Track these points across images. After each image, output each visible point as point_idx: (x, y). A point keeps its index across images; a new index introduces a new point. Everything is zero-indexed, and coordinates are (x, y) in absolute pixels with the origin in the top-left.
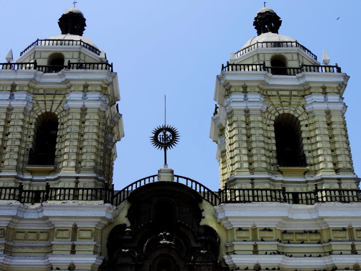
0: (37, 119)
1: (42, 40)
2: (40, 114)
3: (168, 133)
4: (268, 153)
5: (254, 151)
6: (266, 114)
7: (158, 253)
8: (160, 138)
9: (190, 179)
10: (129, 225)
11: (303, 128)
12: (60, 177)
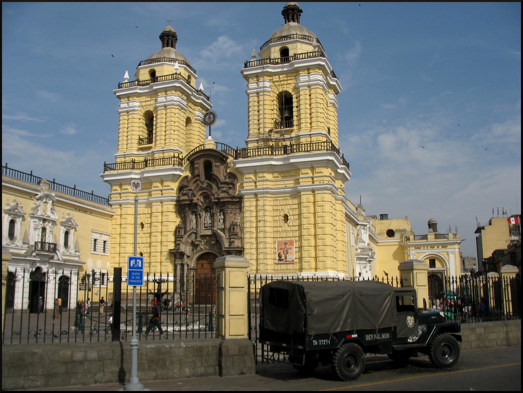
1: (143, 62)
2: (144, 112)
3: (211, 116)
7: (201, 192)
8: (207, 119)
9: (223, 144)
10: (190, 176)
12: (154, 152)
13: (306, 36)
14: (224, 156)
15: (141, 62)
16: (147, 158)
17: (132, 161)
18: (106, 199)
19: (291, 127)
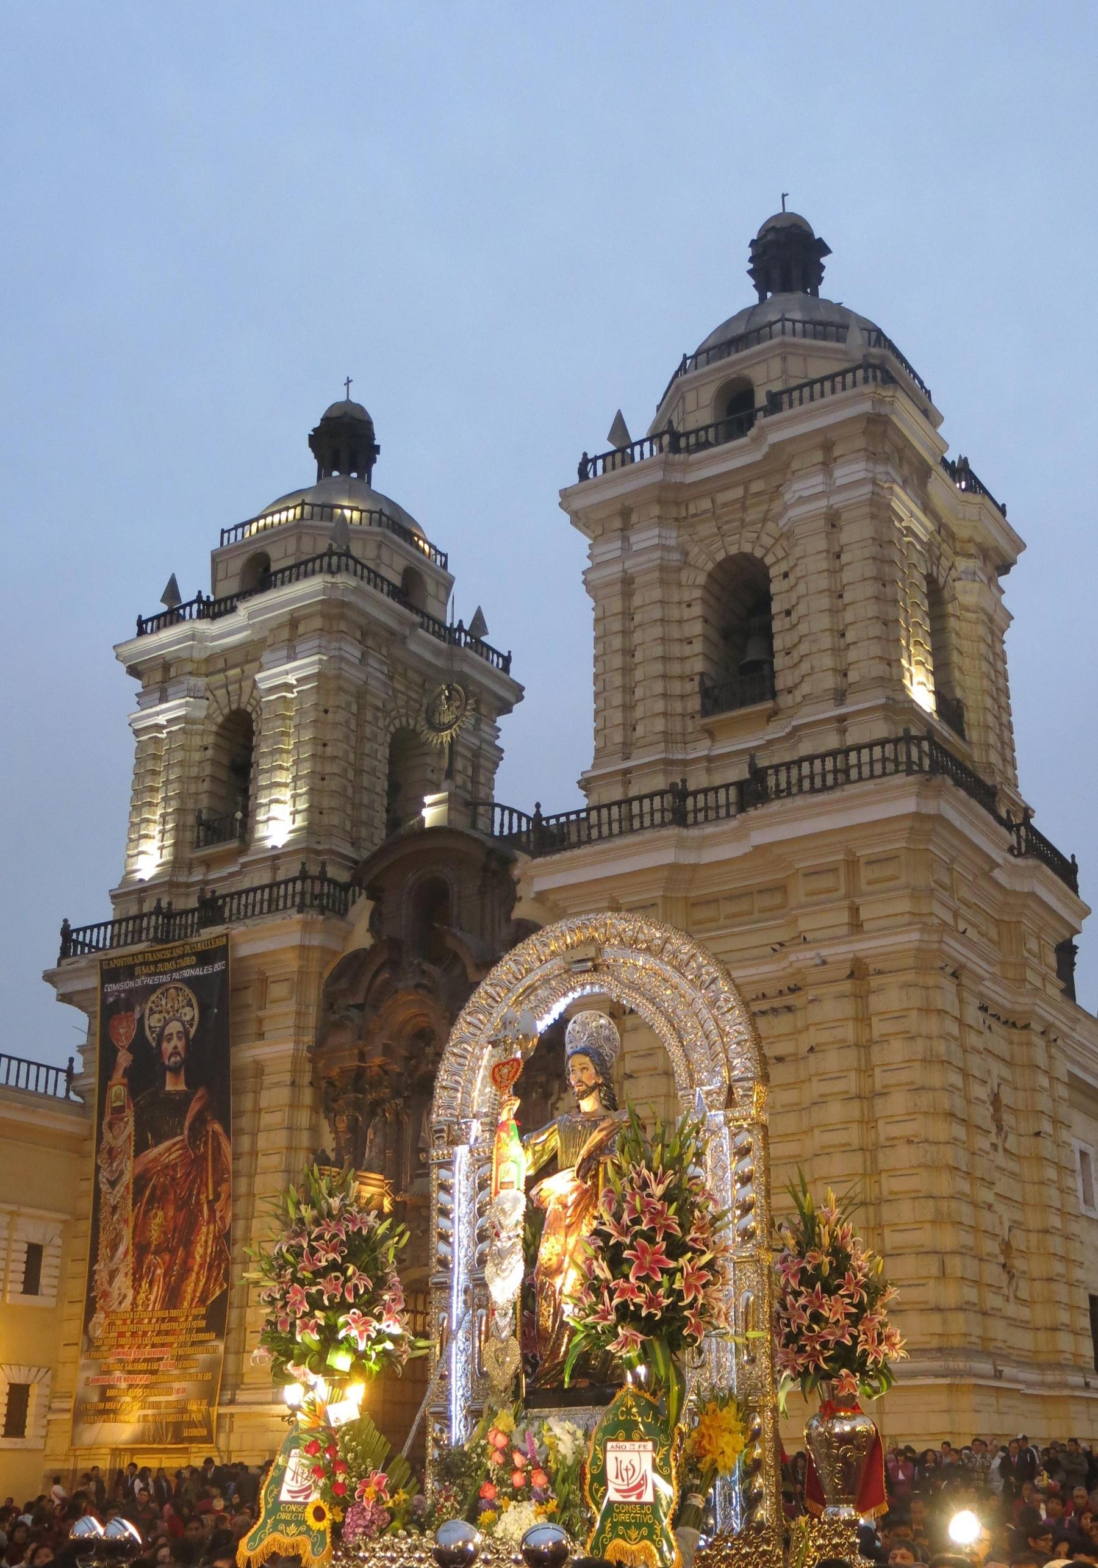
0: (217, 734)
1: (229, 531)
4: (676, 688)
5: (639, 692)
6: (684, 576)
11: (774, 588)
13: (825, 324)
14: (490, 852)
15: (223, 532)
16: (214, 892)
17: (158, 911)
18: (58, 1070)
19: (762, 698)
